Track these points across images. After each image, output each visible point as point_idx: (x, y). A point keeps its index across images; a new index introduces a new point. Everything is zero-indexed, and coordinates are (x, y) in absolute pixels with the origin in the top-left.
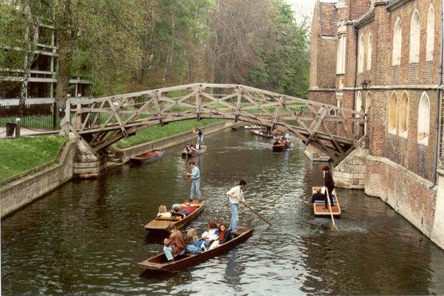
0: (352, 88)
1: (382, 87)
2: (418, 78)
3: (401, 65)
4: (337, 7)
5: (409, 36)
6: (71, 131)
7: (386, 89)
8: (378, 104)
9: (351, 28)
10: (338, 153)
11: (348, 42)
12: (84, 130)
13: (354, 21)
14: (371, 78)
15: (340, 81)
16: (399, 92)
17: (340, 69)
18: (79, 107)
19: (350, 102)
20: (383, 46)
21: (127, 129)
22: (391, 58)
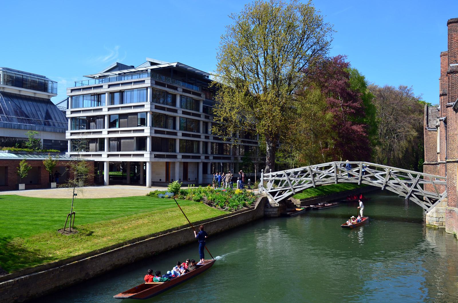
6: (263, 190)
8: (451, 172)
9: (442, 123)
11: (441, 131)
12: (271, 189)
15: (439, 157)
17: (438, 151)
18: (270, 176)
19: (443, 170)
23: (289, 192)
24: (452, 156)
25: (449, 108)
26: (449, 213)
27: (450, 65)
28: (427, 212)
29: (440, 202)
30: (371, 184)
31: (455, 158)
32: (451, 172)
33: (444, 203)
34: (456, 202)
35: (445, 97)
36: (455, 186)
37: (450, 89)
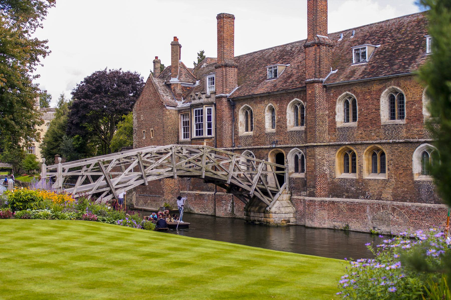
0: (231, 148)
1: (325, 144)
2: (405, 135)
3: (358, 127)
4: (171, 83)
5: (379, 106)
7: (326, 146)
8: (319, 157)
9: (224, 100)
10: (270, 199)
13: (228, 95)
14: (276, 139)
16: (357, 147)
20: (321, 113)
21: (116, 189)
22: (334, 122)
23: (108, 195)
24: (322, 139)
25: (316, 85)
26: (319, 204)
27: (317, 35)
28: (270, 208)
29: (280, 195)
30: (215, 177)
31: (325, 141)
32: (319, 157)
33: (285, 195)
34: (327, 191)
35: (228, 69)
36: (326, 173)
37: (317, 62)
